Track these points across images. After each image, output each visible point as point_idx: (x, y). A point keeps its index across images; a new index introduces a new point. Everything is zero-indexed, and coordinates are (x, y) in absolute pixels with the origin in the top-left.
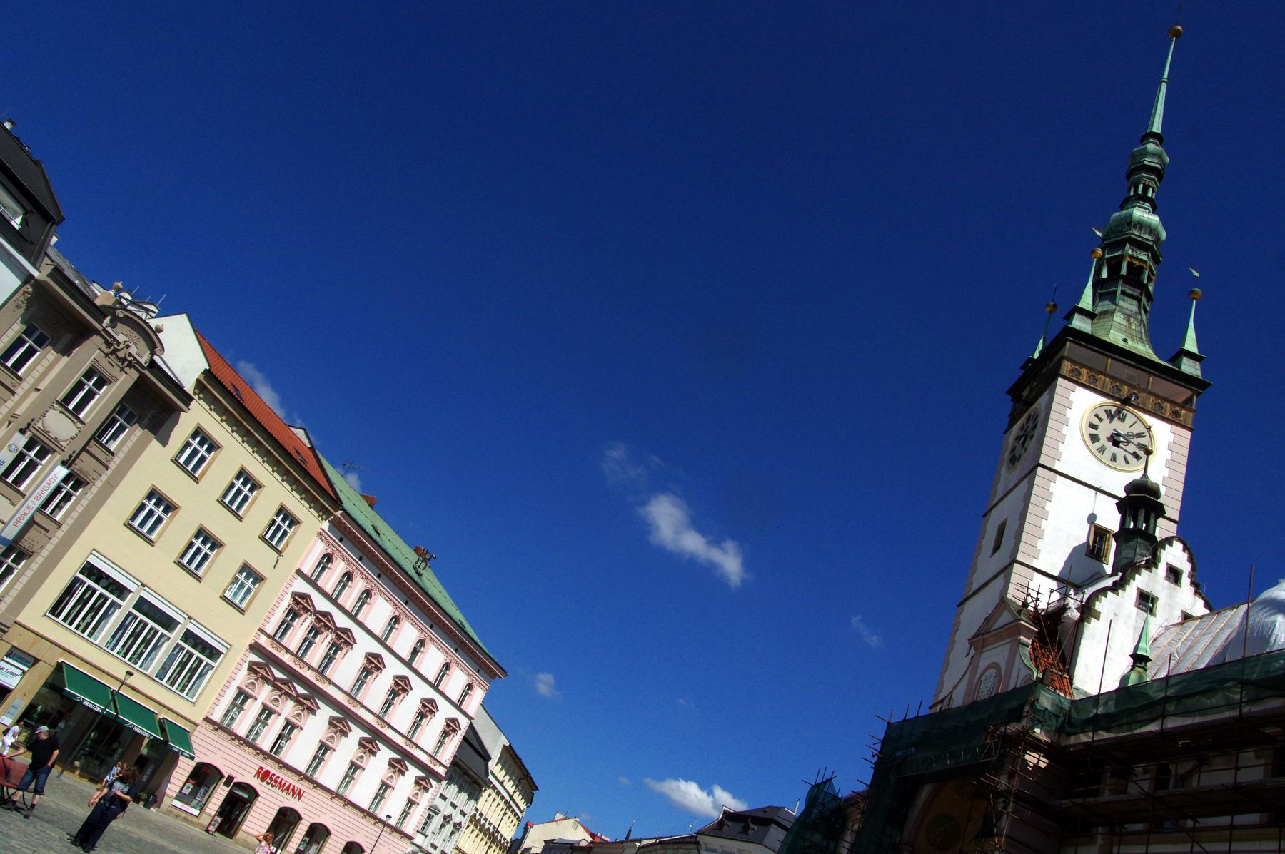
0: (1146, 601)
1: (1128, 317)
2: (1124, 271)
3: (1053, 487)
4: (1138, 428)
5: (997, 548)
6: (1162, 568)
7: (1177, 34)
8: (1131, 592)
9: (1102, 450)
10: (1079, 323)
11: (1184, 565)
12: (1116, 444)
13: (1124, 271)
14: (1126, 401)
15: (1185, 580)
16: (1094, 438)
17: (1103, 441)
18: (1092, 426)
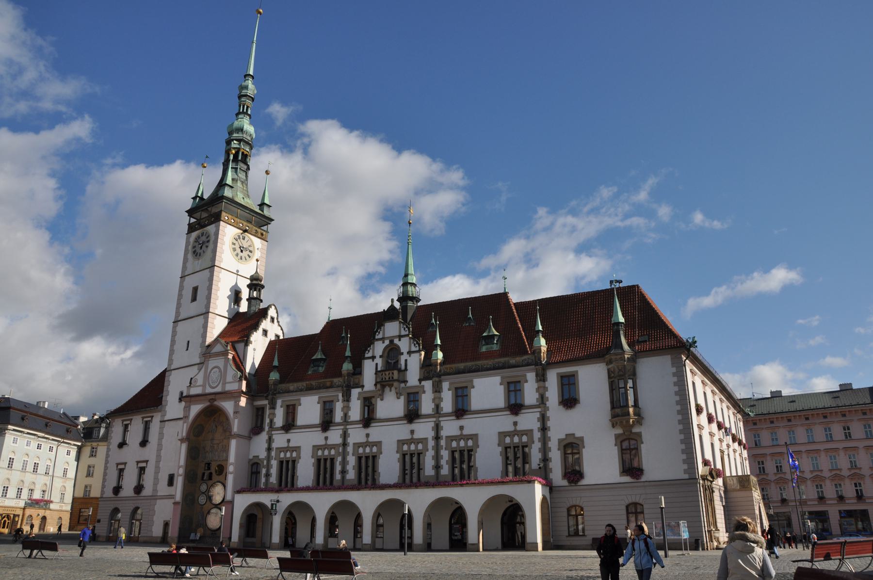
0: (265, 332)
1: (242, 183)
2: (240, 158)
3: (221, 275)
4: (249, 243)
5: (194, 299)
6: (269, 317)
7: (260, 13)
8: (260, 331)
9: (237, 255)
10: (227, 193)
11: (275, 316)
12: (242, 251)
13: (240, 158)
14: (245, 231)
15: (275, 321)
16: (234, 250)
17: (239, 250)
18: (234, 244)
